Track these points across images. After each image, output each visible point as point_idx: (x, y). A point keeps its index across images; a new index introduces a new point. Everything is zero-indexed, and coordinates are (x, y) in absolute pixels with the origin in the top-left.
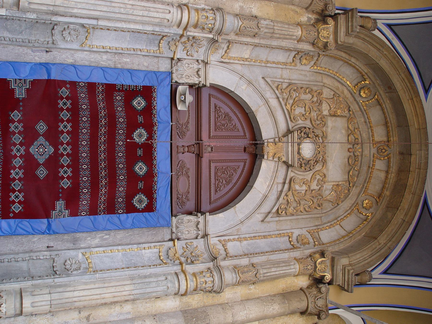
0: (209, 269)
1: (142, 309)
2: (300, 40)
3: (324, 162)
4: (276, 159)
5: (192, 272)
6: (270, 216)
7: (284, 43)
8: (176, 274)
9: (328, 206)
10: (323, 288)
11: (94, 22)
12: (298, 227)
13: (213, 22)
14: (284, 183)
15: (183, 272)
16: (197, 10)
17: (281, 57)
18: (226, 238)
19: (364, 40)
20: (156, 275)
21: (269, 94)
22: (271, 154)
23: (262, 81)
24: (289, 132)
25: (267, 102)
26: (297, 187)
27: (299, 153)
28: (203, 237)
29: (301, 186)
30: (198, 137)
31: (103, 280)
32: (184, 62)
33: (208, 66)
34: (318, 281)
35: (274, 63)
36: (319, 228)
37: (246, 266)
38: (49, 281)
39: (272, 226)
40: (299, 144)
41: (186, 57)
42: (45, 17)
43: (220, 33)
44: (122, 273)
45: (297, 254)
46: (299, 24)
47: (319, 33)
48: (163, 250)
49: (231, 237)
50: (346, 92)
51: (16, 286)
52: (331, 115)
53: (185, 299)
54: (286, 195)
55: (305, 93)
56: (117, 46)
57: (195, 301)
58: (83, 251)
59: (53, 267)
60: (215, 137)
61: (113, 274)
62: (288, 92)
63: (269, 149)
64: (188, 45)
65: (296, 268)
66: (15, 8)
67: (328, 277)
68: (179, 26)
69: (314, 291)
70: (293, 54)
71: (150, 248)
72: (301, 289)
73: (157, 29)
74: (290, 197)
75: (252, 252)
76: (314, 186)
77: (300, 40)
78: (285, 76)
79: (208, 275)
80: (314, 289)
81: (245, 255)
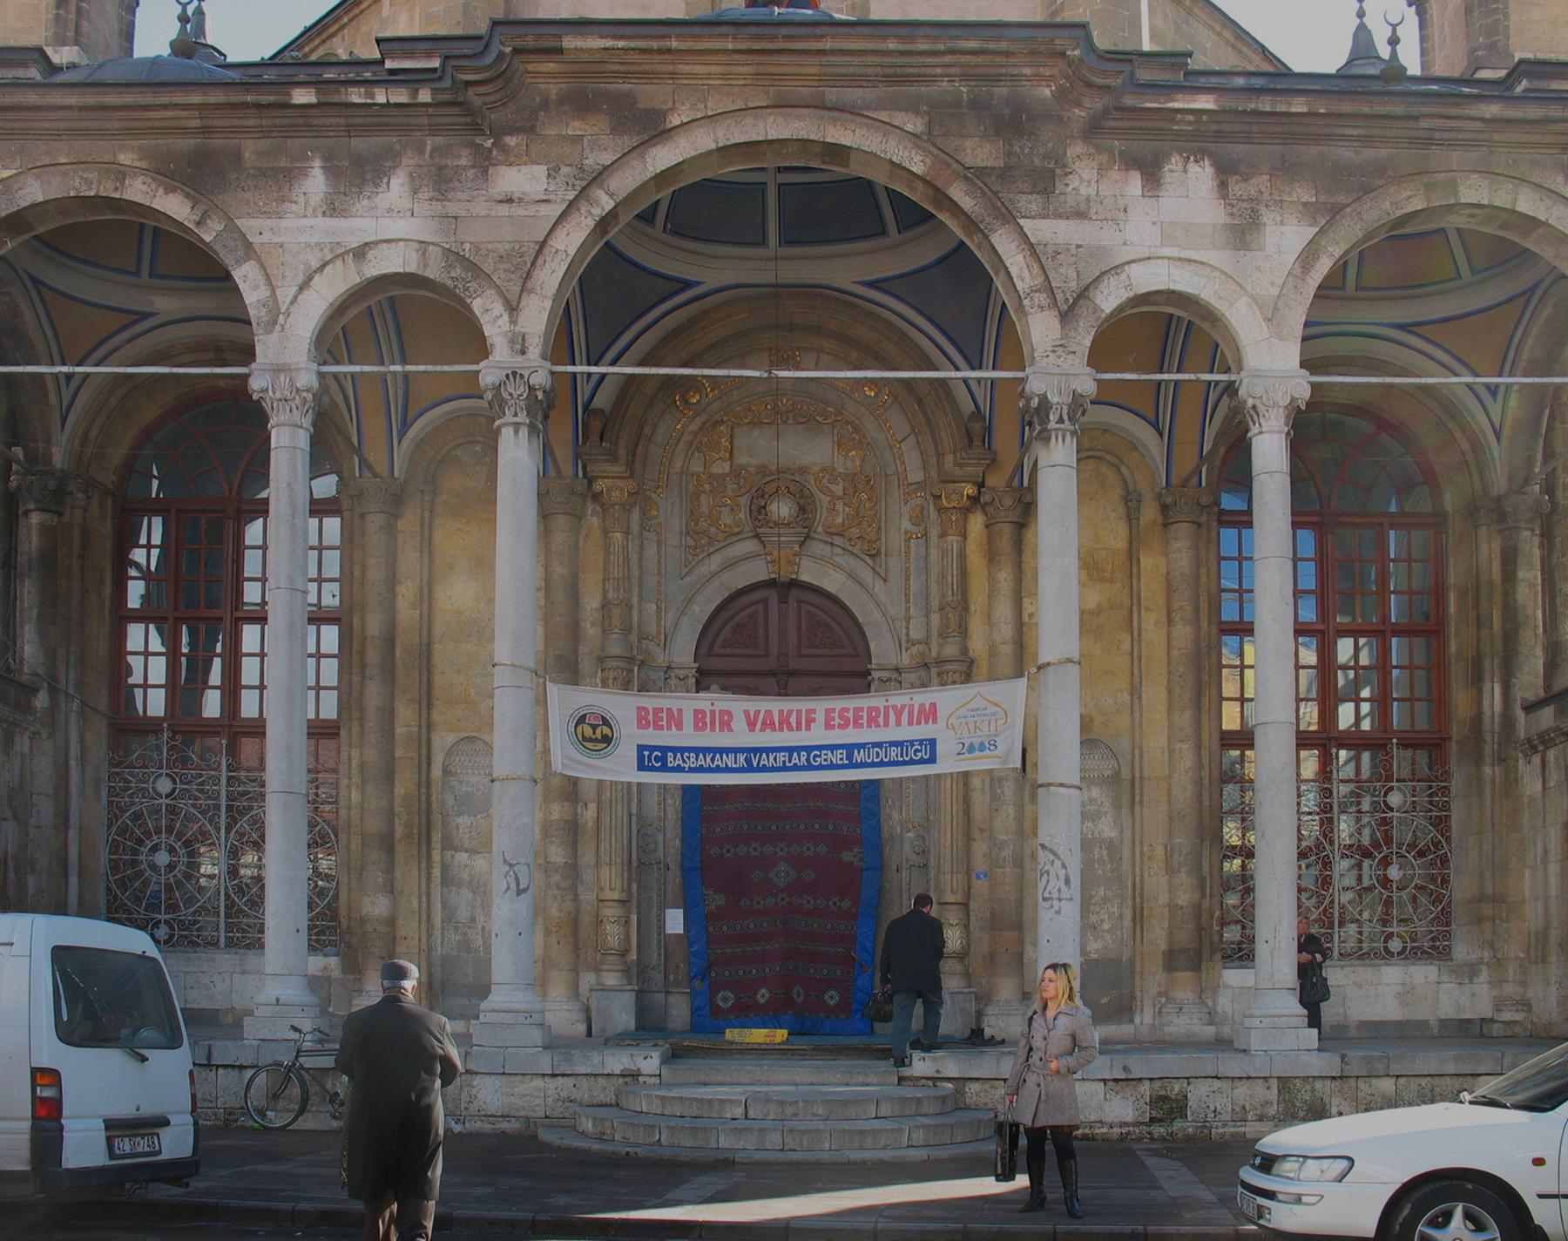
10: (985, 498)
17: (651, 551)
24: (757, 536)
34: (975, 500)
45: (934, 533)
46: (606, 532)
65: (953, 539)
67: (969, 490)
69: (990, 509)
76: (838, 490)
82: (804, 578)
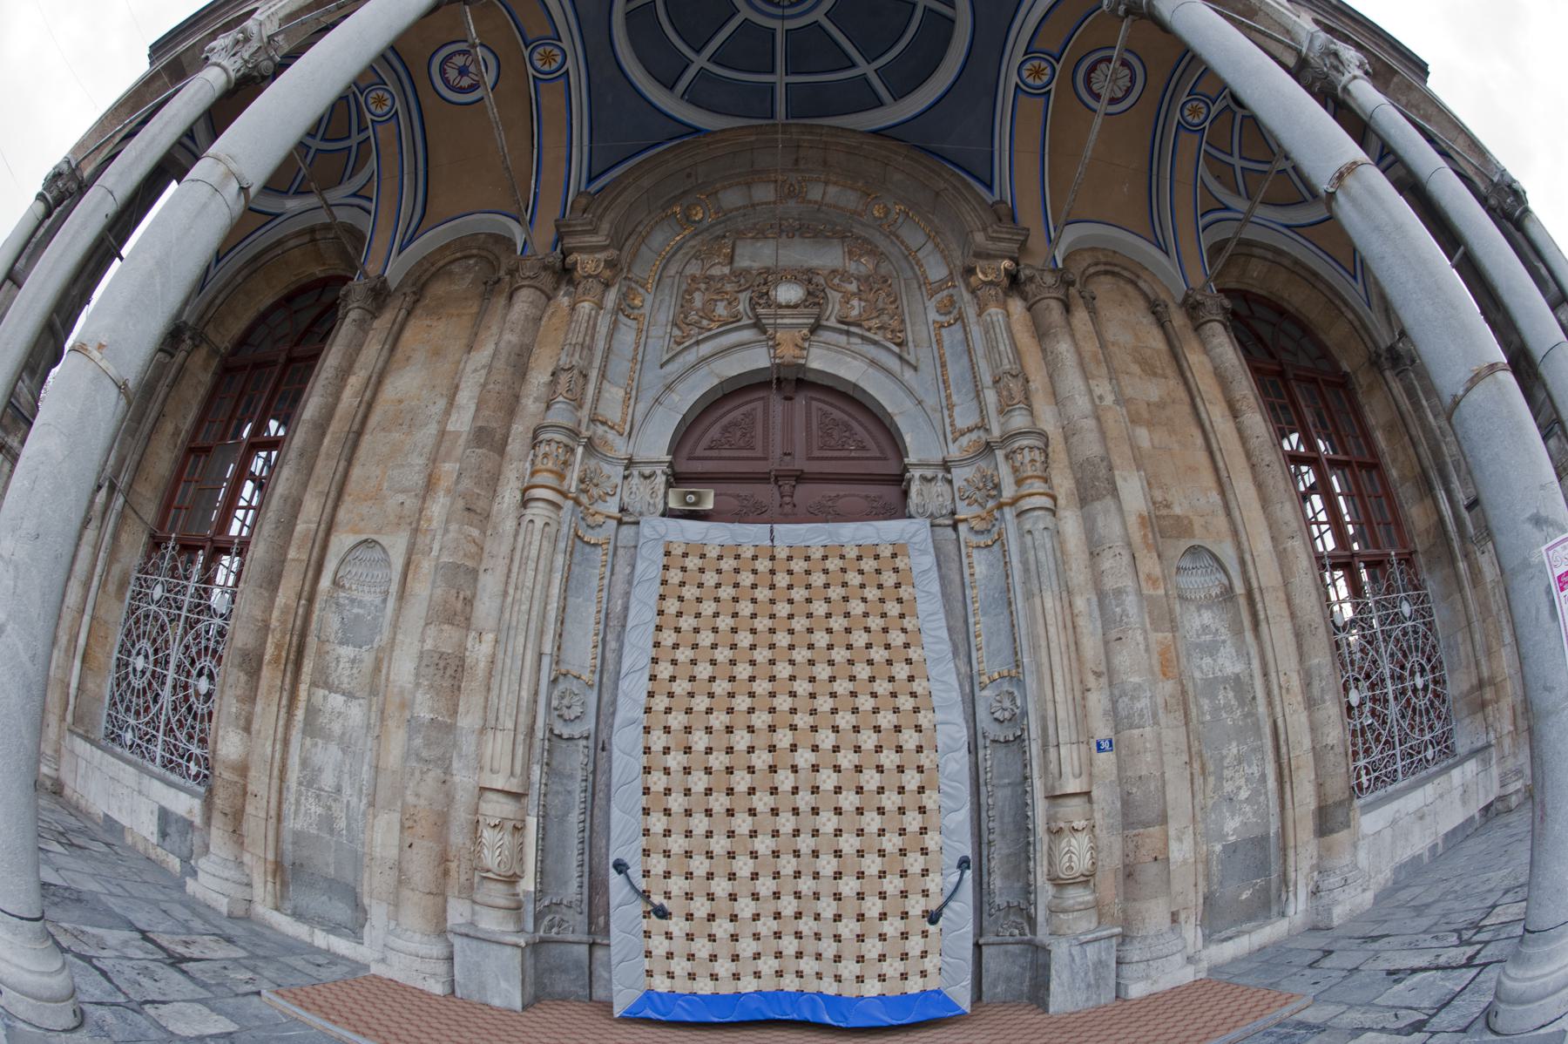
0: (1007, 457)
1: (1082, 578)
2: (600, 306)
3: (810, 270)
4: (806, 345)
5: (1014, 487)
6: (906, 356)
7: (603, 329)
8: (1020, 514)
9: (885, 268)
11: (546, 661)
12: (923, 316)
13: (554, 446)
14: (848, 333)
15: (1014, 502)
16: (533, 474)
18: (948, 429)
19: (606, 209)
20: (1023, 551)
21: (690, 357)
22: (797, 352)
23: (669, 368)
24: (758, 325)
25: (705, 359)
26: (855, 313)
27: (796, 306)
28: (948, 470)
29: (853, 307)
30: (763, 478)
31: (1035, 648)
32: (626, 499)
33: (636, 459)
35: (636, 349)
36: (923, 282)
37: (999, 394)
38: (1035, 748)
39: (923, 355)
40: (780, 306)
41: (617, 498)
42: (537, 750)
43: (574, 433)
44: (1021, 614)
45: (971, 312)
47: (590, 276)
48: (974, 540)
49: (947, 421)
50: (692, 243)
51: (1040, 807)
52: (731, 261)
53: (1062, 502)
54: (869, 330)
55: (691, 301)
56: (592, 621)
57: (1064, 483)
58: (977, 688)
59: (1007, 742)
60: (765, 447)
61: (1023, 632)
62: (689, 327)
63: (788, 353)
64: (595, 492)
65: (994, 311)
66: (525, 801)
67: (1006, 263)
68: (558, 507)
70: (622, 317)
71: (971, 566)
72: (1029, 309)
73: (562, 545)
74: (875, 323)
75: (970, 385)
76: (853, 287)
77: (600, 306)
78: (661, 333)
79: (1019, 457)
80: (1027, 288)
81: (978, 396)
82: (815, 364)
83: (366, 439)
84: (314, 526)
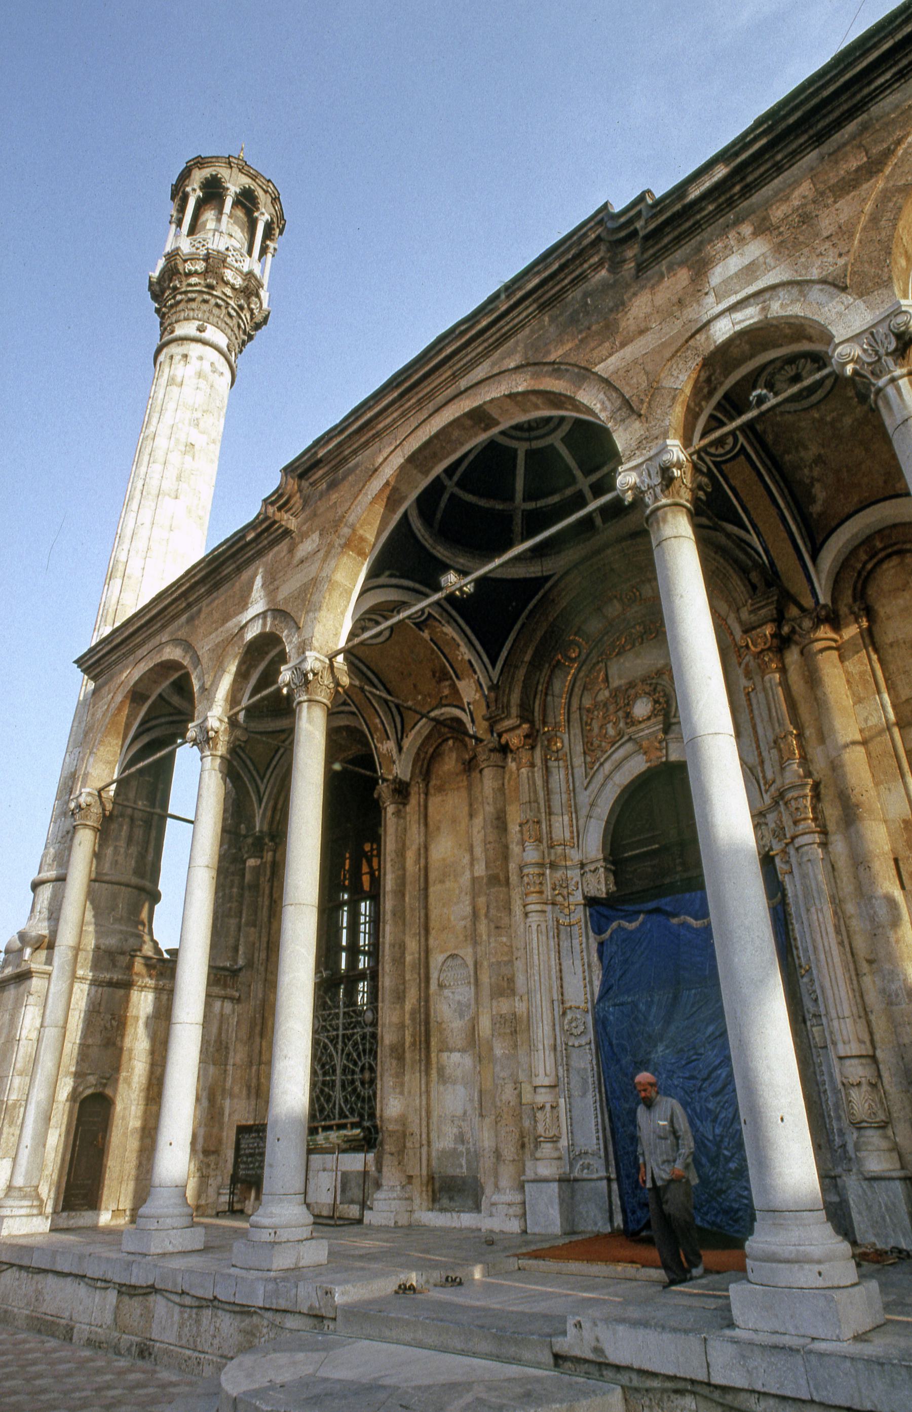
11: (556, 1004)
19: (509, 694)
68: (543, 912)
77: (532, 765)
83: (431, 889)
84: (417, 956)
